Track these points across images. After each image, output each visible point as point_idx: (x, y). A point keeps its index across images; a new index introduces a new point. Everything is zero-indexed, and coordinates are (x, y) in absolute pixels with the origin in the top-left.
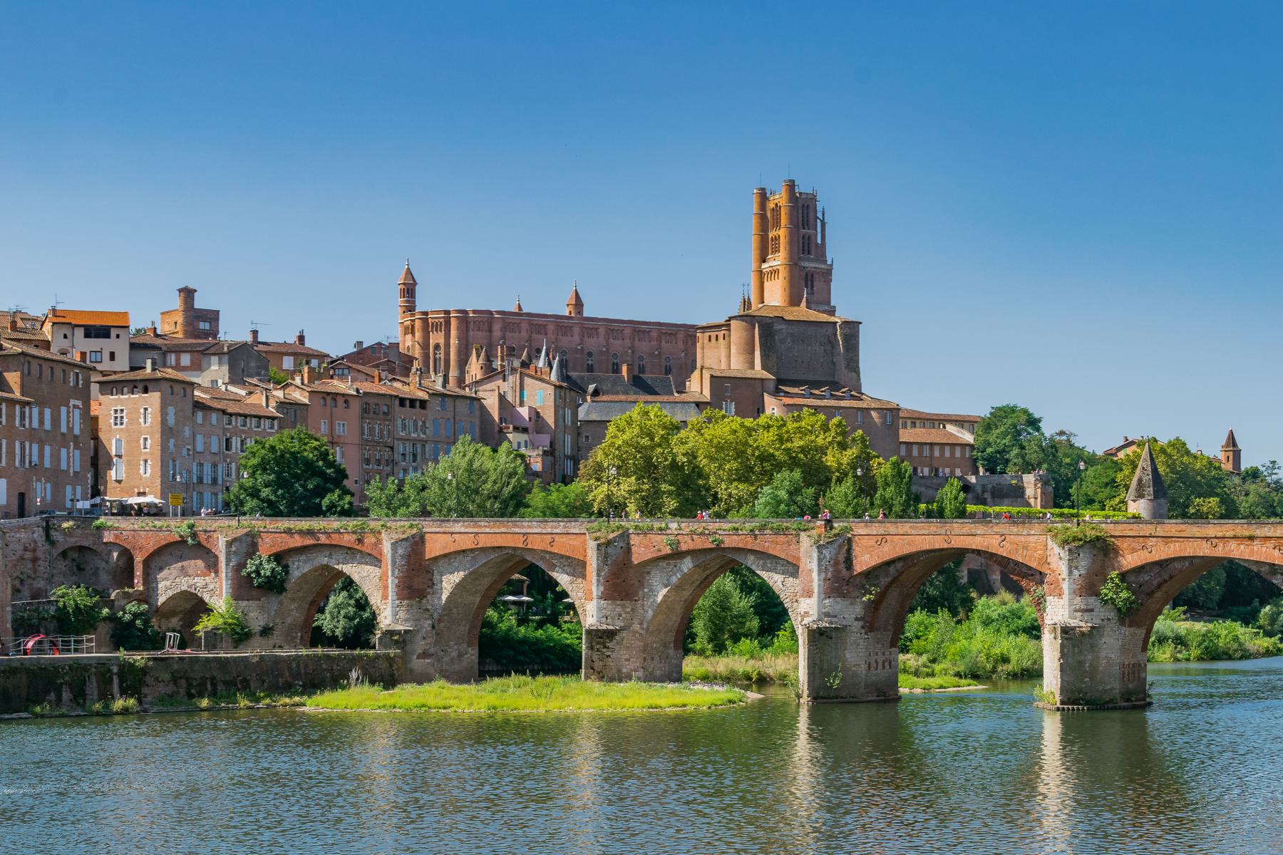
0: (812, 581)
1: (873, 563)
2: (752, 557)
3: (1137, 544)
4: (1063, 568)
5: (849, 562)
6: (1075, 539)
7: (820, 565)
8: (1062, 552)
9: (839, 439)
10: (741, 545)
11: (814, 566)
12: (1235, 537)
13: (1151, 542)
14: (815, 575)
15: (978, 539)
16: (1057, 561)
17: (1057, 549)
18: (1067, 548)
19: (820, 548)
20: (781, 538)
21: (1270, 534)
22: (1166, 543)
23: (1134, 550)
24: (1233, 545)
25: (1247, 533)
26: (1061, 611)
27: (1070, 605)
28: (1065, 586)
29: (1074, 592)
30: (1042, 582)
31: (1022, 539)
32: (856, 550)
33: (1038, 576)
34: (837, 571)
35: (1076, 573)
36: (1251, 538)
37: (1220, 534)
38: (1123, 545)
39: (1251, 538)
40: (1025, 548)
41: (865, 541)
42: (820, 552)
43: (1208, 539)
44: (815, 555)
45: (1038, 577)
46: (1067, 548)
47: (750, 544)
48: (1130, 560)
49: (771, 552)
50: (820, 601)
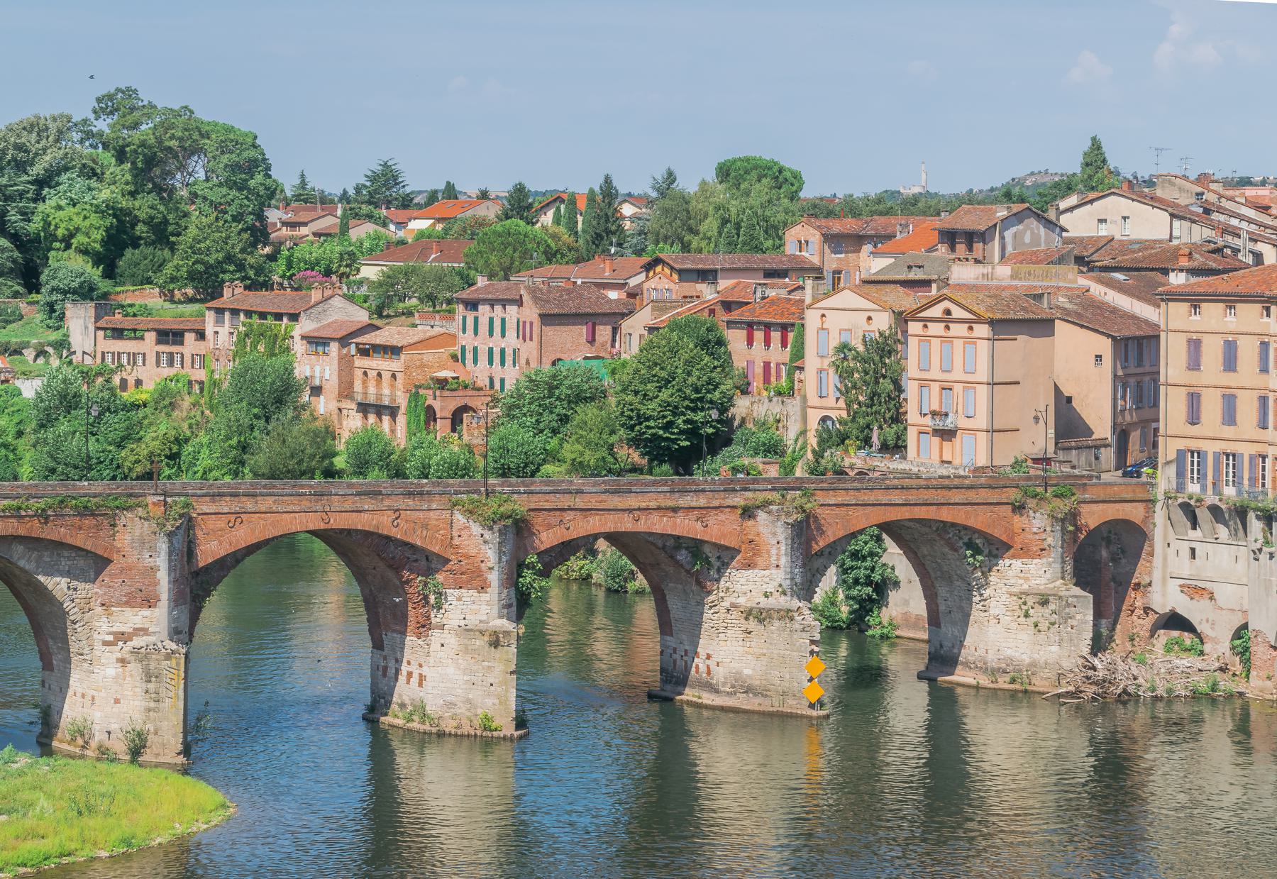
0: (157, 583)
1: (223, 553)
2: (20, 548)
3: (554, 518)
4: (491, 554)
5: (190, 552)
6: (503, 517)
7: (170, 561)
8: (488, 535)
9: (554, 424)
10: (22, 532)
11: (162, 561)
12: (659, 508)
13: (568, 516)
14: (163, 577)
15: (365, 516)
16: (481, 545)
17: (476, 529)
18: (496, 527)
19: (170, 535)
20: (88, 521)
21: (694, 504)
22: (586, 517)
23: (549, 526)
24: (655, 517)
25: (670, 503)
26: (484, 609)
27: (500, 600)
28: (494, 578)
29: (503, 585)
30: (429, 572)
31: (421, 515)
32: (199, 533)
33: (428, 562)
34: (182, 568)
35: (504, 559)
36: (675, 510)
37: (644, 505)
38: (538, 520)
39: (675, 510)
40: (426, 527)
41: (212, 523)
42: (170, 542)
43: (630, 511)
44: (163, 546)
45: (424, 562)
46: (496, 527)
47: (35, 529)
48: (547, 538)
49: (70, 541)
50: (170, 613)
